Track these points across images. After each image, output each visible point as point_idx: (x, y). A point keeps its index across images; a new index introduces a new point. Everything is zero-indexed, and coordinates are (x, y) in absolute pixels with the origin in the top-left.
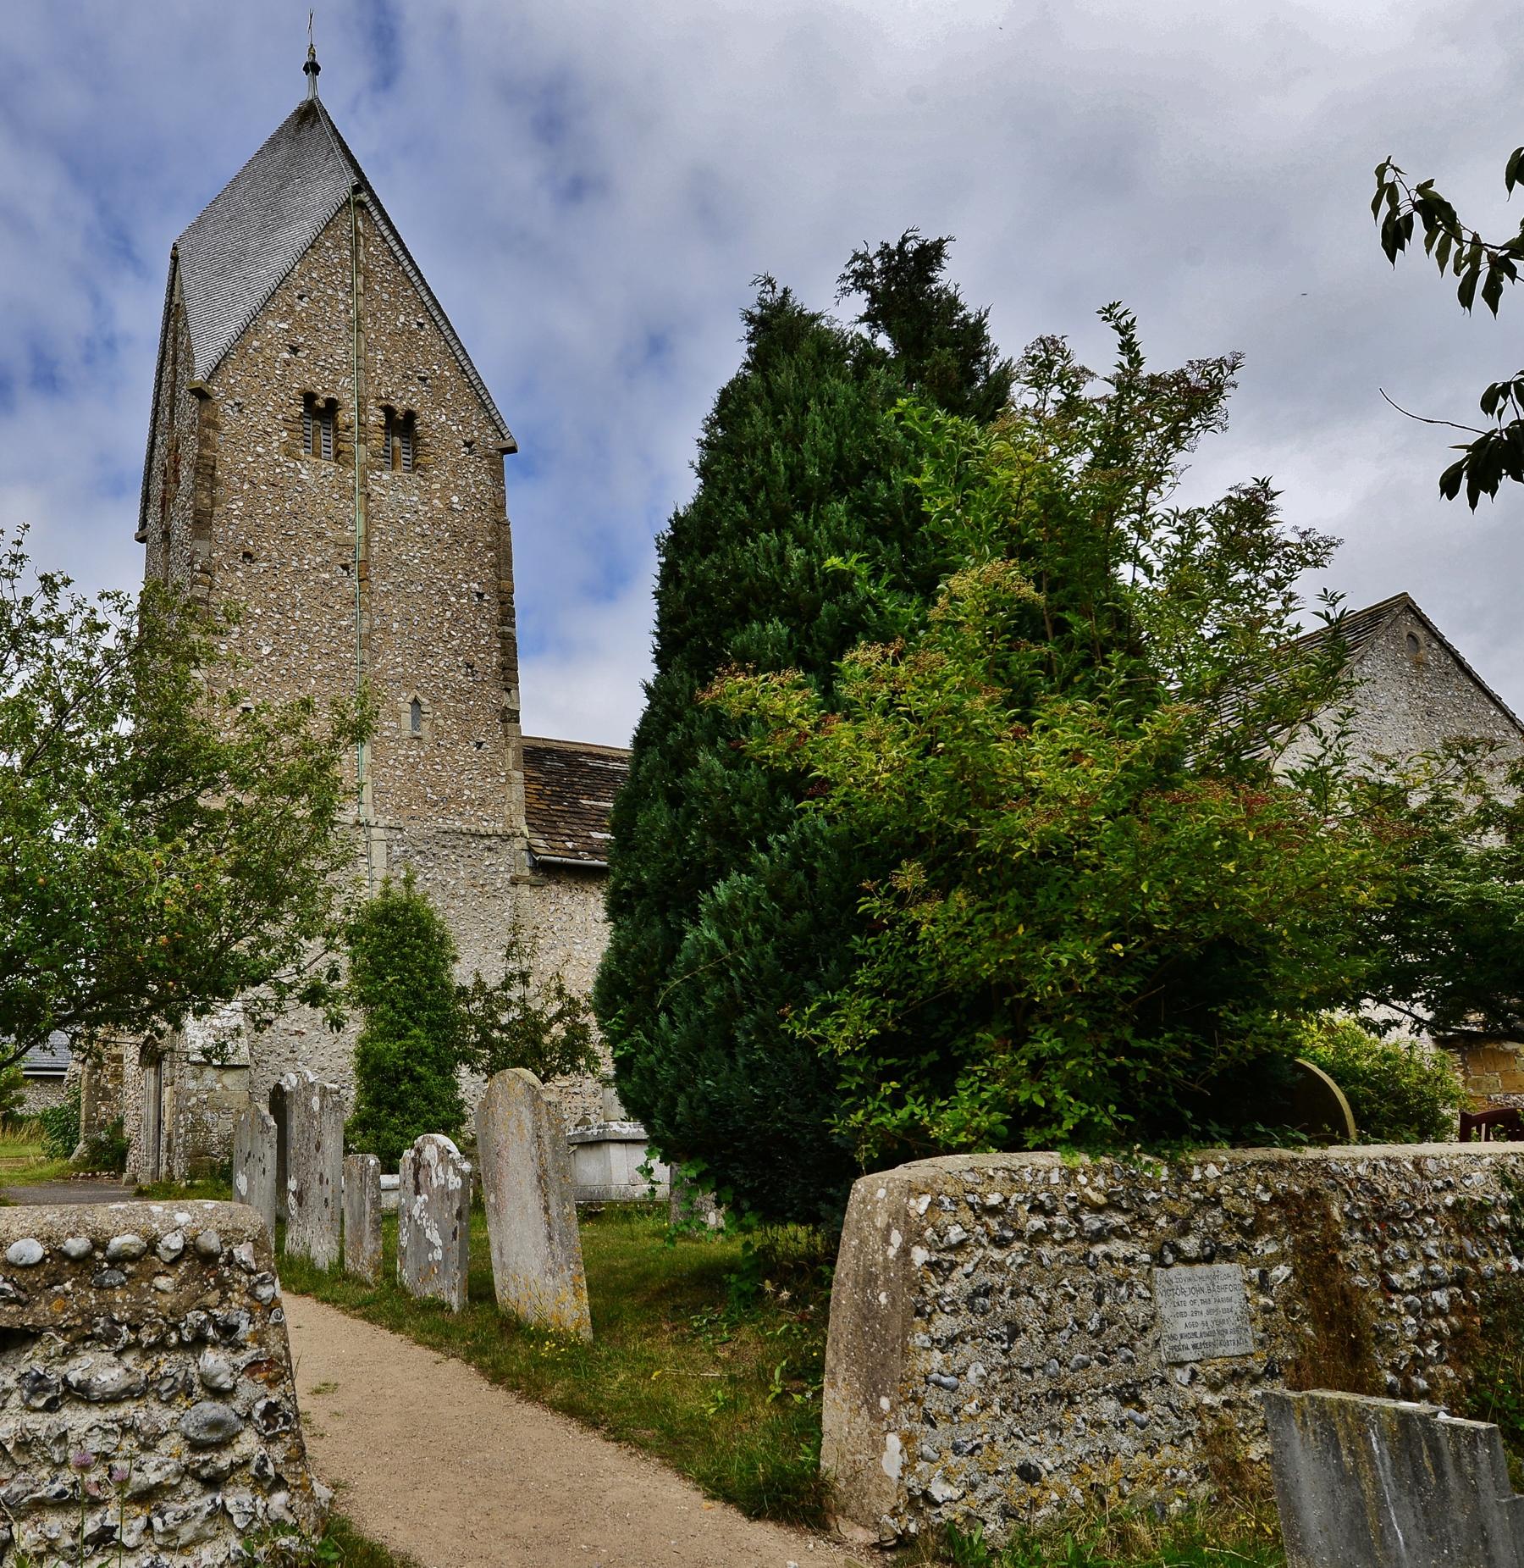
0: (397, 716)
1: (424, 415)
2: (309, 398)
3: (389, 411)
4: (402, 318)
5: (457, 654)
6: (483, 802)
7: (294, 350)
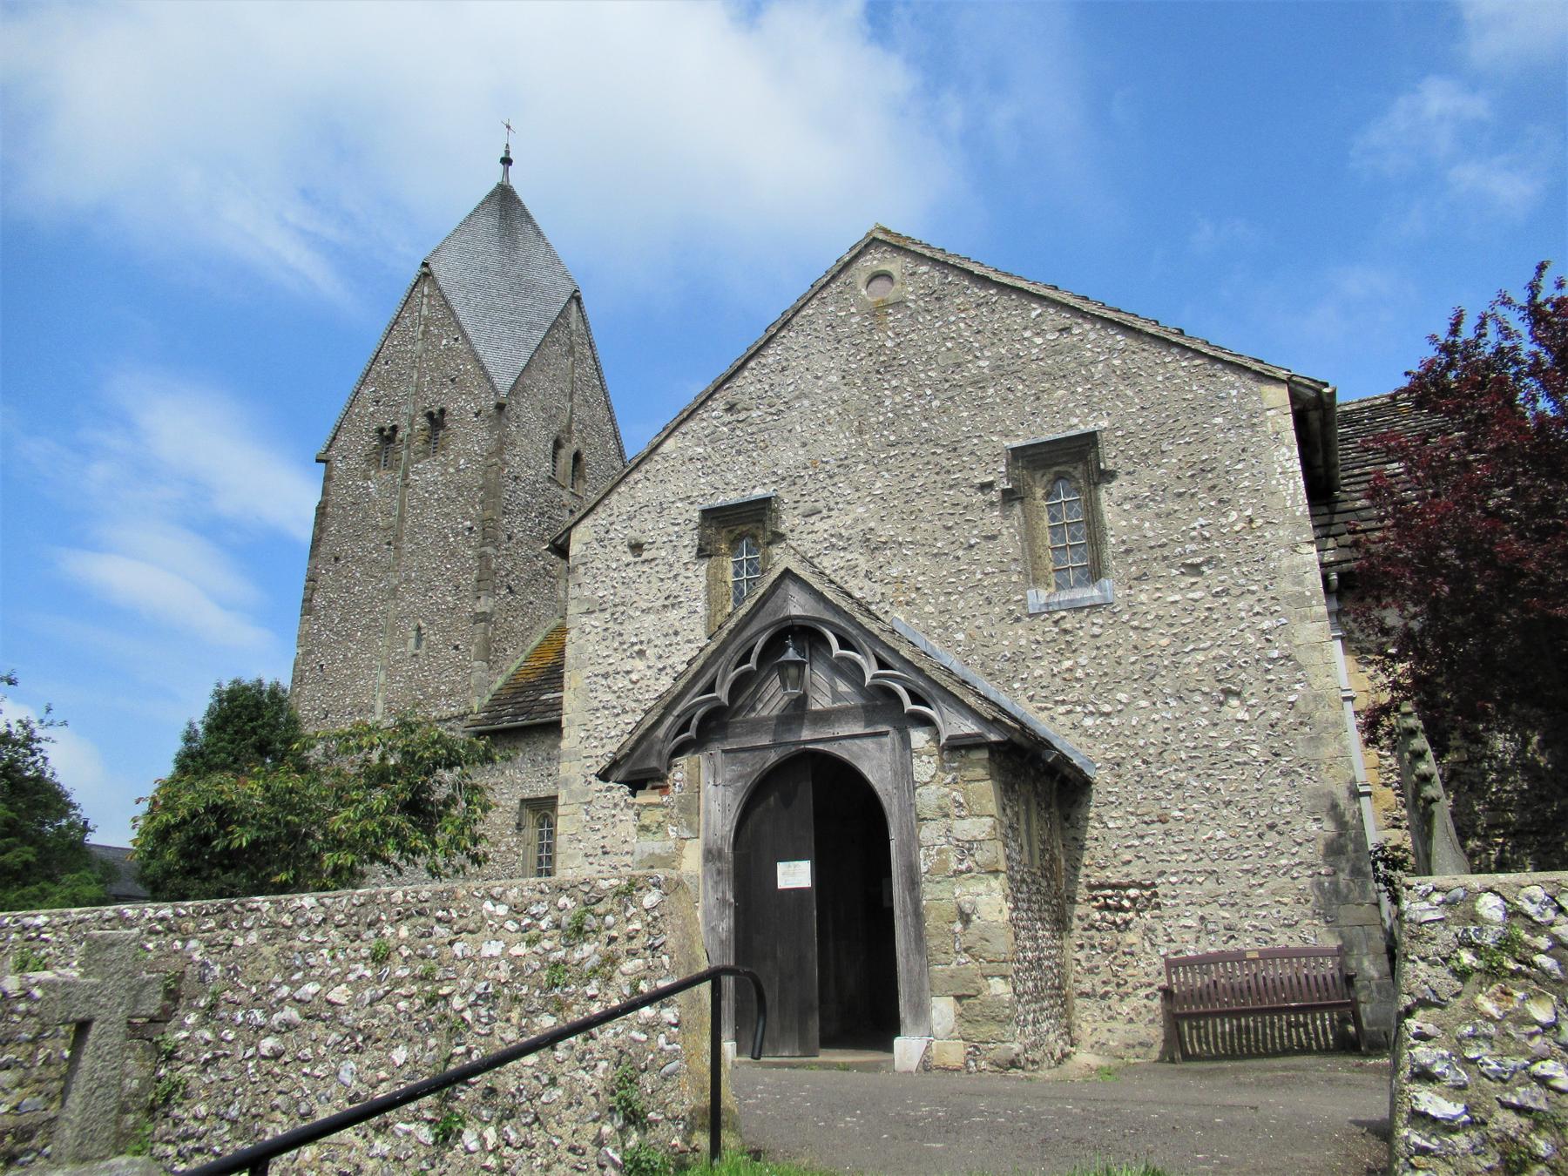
0: (405, 644)
1: (451, 407)
3: (430, 415)
6: (452, 694)
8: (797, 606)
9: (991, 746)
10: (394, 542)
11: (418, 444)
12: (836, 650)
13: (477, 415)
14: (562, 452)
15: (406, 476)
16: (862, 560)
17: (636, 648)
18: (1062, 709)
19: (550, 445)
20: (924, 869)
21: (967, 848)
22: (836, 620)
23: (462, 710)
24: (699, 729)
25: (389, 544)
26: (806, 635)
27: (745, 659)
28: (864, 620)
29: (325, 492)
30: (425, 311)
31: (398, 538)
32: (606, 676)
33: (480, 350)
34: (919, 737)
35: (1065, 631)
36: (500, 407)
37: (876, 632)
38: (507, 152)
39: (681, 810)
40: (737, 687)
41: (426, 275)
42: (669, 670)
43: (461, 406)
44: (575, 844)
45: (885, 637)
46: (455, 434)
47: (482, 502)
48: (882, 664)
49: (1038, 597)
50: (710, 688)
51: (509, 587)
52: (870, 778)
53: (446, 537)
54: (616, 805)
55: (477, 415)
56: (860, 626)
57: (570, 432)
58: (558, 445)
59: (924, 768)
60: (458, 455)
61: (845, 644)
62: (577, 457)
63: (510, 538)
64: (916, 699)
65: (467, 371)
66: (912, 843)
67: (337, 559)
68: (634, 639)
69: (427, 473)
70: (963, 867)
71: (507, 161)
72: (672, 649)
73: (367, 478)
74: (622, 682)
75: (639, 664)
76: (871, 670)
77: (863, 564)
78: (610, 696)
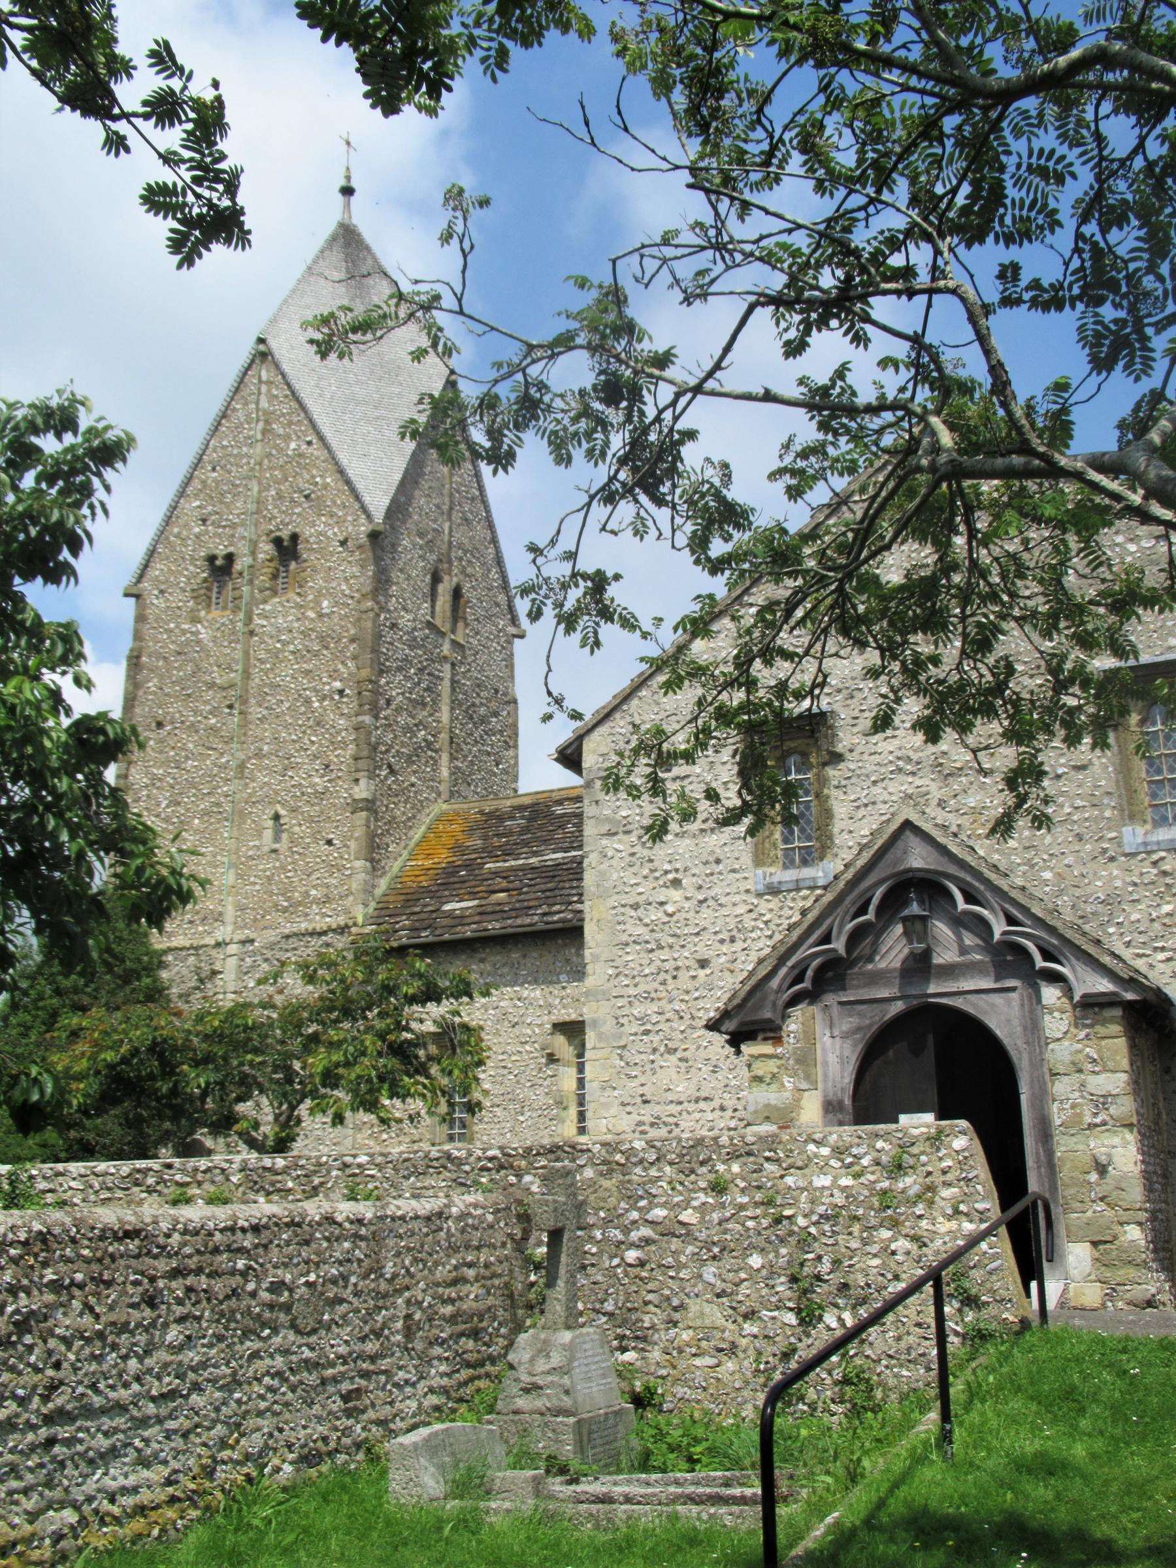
0: (259, 834)
1: (307, 532)
2: (211, 559)
3: (278, 542)
4: (293, 445)
5: (316, 757)
6: (328, 900)
7: (204, 521)
8: (918, 858)
9: (1128, 1006)
10: (238, 703)
11: (263, 579)
12: (962, 905)
13: (343, 543)
14: (441, 588)
15: (249, 620)
16: (933, 787)
17: (670, 876)
18: (1161, 956)
19: (428, 578)
20: (1058, 1122)
21: (1102, 1101)
22: (962, 874)
23: (341, 920)
24: (816, 980)
25: (231, 707)
26: (929, 887)
27: (862, 910)
28: (992, 876)
29: (138, 636)
30: (264, 404)
31: (244, 702)
32: (636, 906)
33: (343, 458)
34: (1050, 994)
35: (1165, 873)
36: (374, 536)
37: (1006, 888)
38: (348, 178)
39: (798, 1061)
40: (855, 938)
41: (263, 354)
42: (711, 902)
43: (317, 531)
44: (609, 1092)
45: (1014, 894)
46: (314, 570)
47: (355, 658)
48: (1011, 921)
49: (1133, 835)
50: (826, 939)
51: (390, 766)
52: (998, 1032)
53: (308, 701)
54: (655, 1050)
55: (343, 543)
56: (987, 882)
57: (450, 562)
58: (436, 579)
59: (1056, 1024)
60: (319, 595)
61: (970, 898)
62: (457, 593)
63: (388, 702)
64: (1047, 956)
65: (326, 486)
66: (1042, 1097)
67: (160, 725)
68: (667, 867)
69: (278, 616)
70: (1098, 1120)
71: (348, 191)
72: (714, 878)
73: (195, 620)
74: (655, 915)
75: (676, 895)
76: (999, 928)
77: (936, 792)
78: (641, 930)
